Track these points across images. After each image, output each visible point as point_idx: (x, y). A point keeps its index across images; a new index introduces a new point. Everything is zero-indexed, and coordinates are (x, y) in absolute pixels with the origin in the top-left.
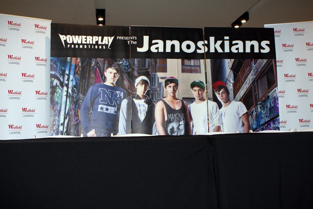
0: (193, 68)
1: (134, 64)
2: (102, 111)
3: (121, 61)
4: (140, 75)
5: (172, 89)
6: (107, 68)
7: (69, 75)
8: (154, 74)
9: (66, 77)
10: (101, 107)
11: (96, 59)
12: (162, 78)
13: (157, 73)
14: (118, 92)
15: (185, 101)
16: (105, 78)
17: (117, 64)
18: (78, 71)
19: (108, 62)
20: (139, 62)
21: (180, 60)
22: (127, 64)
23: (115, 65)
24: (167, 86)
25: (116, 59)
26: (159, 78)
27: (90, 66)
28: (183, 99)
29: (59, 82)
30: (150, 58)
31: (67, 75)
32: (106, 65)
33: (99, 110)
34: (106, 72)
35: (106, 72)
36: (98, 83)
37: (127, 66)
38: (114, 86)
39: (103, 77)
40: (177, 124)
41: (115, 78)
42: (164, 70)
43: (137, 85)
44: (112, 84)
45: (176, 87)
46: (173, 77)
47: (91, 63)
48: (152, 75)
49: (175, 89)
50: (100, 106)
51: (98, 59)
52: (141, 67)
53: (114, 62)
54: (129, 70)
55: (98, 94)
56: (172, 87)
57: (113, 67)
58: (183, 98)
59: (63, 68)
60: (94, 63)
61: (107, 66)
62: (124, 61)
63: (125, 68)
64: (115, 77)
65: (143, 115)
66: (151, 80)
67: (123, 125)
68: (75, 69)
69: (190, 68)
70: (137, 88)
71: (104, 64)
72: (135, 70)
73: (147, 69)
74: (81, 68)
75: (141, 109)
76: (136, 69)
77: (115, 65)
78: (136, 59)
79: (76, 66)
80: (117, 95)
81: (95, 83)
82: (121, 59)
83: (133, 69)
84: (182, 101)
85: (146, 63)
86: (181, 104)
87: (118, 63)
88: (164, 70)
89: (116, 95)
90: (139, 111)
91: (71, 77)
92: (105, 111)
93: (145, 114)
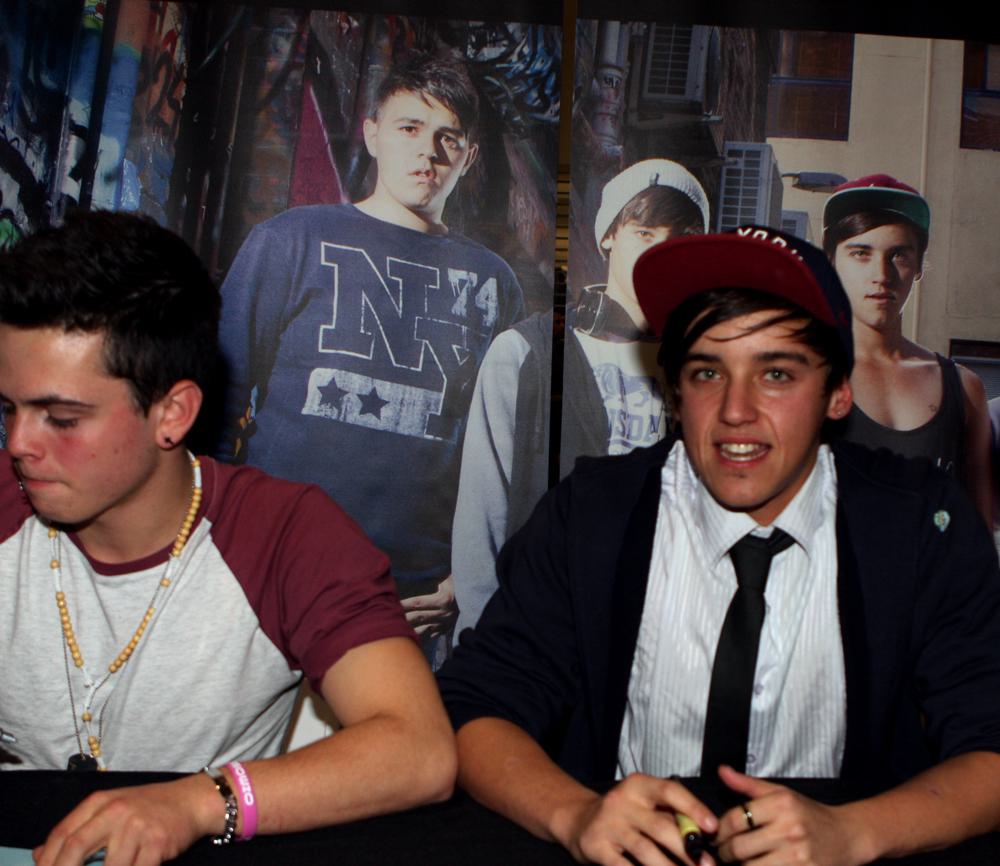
1: (599, 63)
2: (331, 413)
3: (495, 43)
4: (639, 151)
5: (874, 268)
6: (387, 89)
7: (90, 137)
8: (751, 145)
9: (72, 147)
10: (325, 383)
11: (303, 21)
12: (806, 182)
13: (770, 141)
14: (462, 274)
15: (965, 364)
16: (368, 164)
17: (467, 62)
18: (160, 102)
19: (397, 47)
20: (638, 59)
21: (953, 50)
22: (538, 66)
23: (444, 71)
25: (455, 24)
26: (787, 182)
27: (256, 74)
28: (951, 353)
29: (16, 187)
30: (723, 24)
31: (77, 130)
32: (378, 70)
33: (312, 406)
34: (375, 119)
35: (375, 119)
36: (311, 200)
37: (539, 80)
38: (433, 229)
39: (355, 161)
41: (442, 169)
42: (828, 118)
43: (612, 230)
44: (417, 210)
45: (912, 256)
47: (262, 50)
48: (732, 153)
49: (902, 272)
50: (320, 377)
51: (322, 22)
52: (651, 90)
53: (441, 45)
54: (547, 116)
55: (305, 287)
56: (877, 257)
57: (431, 86)
58: (959, 346)
59: (47, 81)
60: (285, 46)
61: (384, 75)
62: (513, 43)
63: (520, 100)
64: (439, 158)
66: (723, 196)
67: (489, 525)
68: (142, 87)
70: (607, 252)
71: (362, 61)
72: (602, 109)
73: (695, 108)
74: (191, 82)
75: (632, 410)
76: (613, 100)
77: (444, 71)
78: (614, 27)
79: (146, 71)
80: (454, 299)
81: (291, 202)
82: (495, 22)
83: (592, 104)
84: (947, 368)
85: (691, 63)
86: (933, 389)
87: (470, 52)
88: (828, 118)
89: (447, 293)
90: (616, 424)
91: (110, 149)
92: (354, 416)
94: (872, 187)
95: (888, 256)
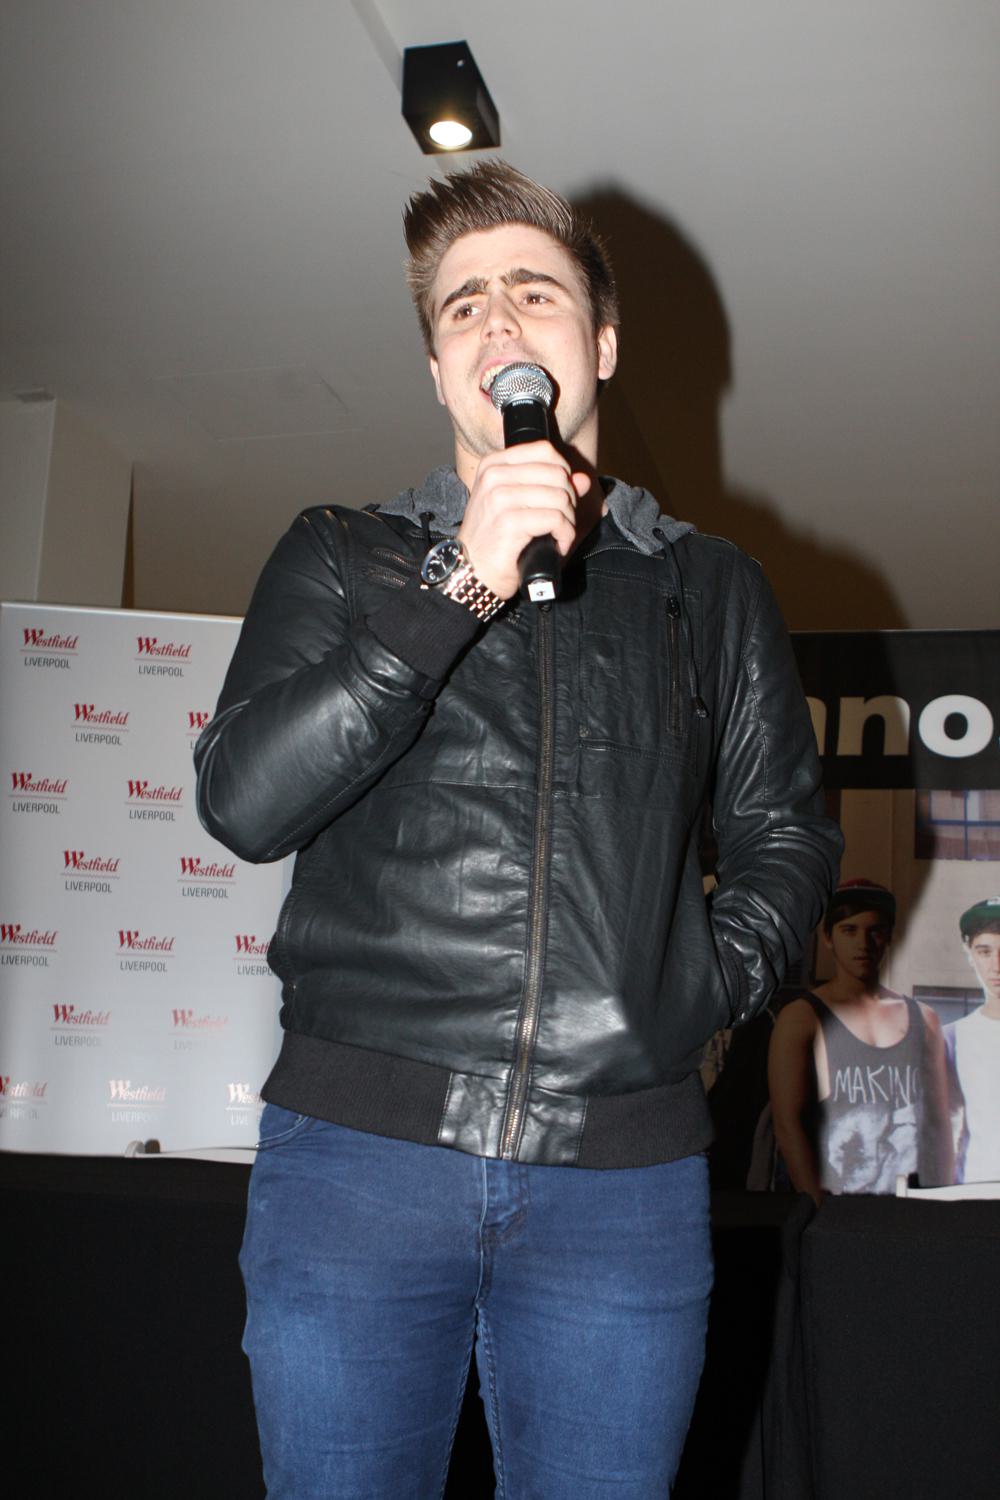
0: (976, 835)
15: (923, 1001)
24: (837, 930)
28: (915, 993)
40: (879, 1120)
46: (867, 883)
56: (861, 934)
58: (921, 990)
65: (711, 1065)
69: (961, 836)
86: (902, 1020)
93: (721, 1062)
94: (856, 887)
95: (869, 930)
